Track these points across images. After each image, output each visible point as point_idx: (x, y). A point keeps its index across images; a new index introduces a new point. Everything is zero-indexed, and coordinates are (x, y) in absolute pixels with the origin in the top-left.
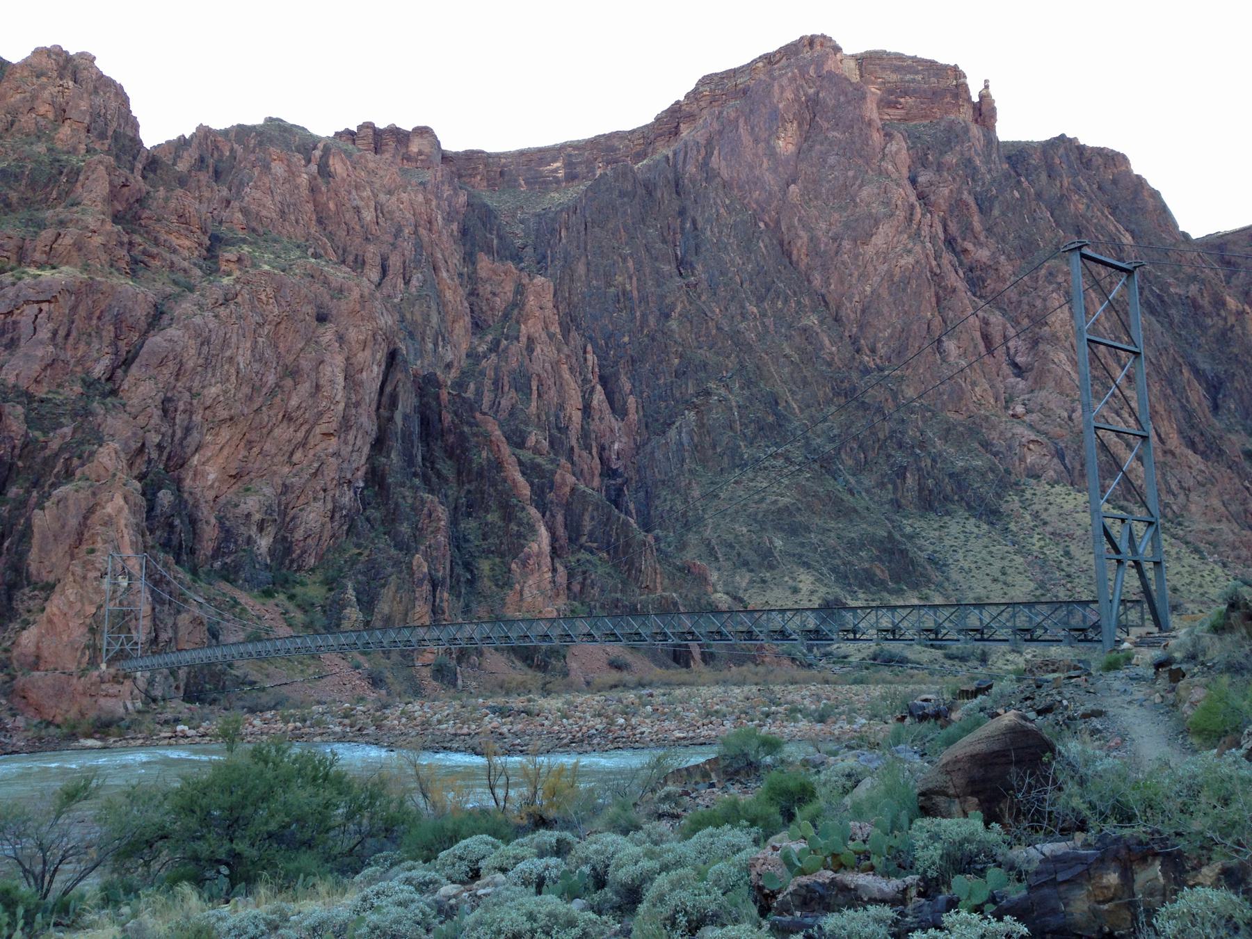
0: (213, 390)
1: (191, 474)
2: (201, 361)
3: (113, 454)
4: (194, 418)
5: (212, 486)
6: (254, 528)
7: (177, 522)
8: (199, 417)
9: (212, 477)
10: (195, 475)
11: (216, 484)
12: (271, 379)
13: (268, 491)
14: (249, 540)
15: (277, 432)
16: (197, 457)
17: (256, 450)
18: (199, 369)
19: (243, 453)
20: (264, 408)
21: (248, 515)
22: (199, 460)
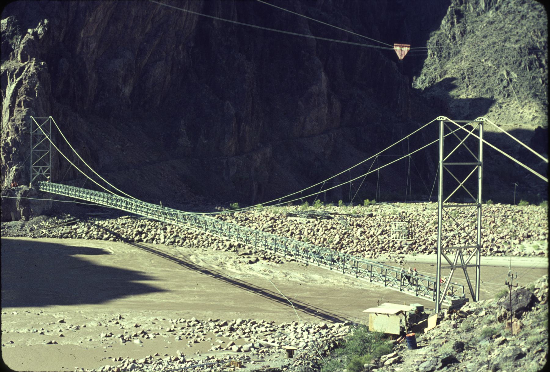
1: (80, 45)
6: (120, 81)
10: (83, 45)
16: (83, 32)
22: (84, 34)
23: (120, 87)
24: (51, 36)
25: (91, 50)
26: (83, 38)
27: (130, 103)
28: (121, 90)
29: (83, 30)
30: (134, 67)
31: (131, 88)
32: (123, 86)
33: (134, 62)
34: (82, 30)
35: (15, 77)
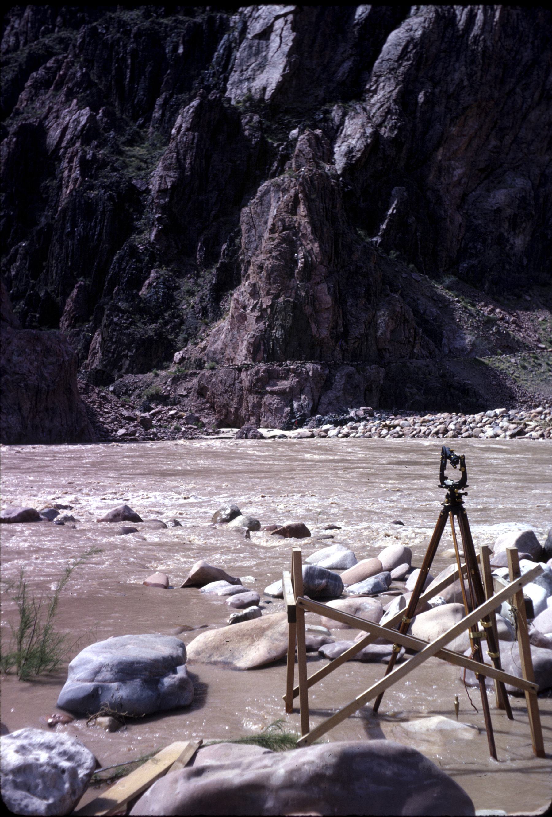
0: (457, 76)
2: (444, 46)
3: (313, 141)
4: (437, 109)
5: (459, 183)
6: (506, 225)
7: (411, 220)
8: (442, 108)
9: (459, 172)
10: (440, 172)
11: (464, 180)
12: (527, 55)
13: (520, 182)
14: (501, 241)
15: (533, 116)
16: (441, 150)
17: (508, 139)
18: (442, 55)
19: (493, 142)
20: (518, 90)
21: (499, 210)
22: (444, 155)
23: (506, 234)
24: (381, 155)
25: (455, 179)
26: (441, 161)
27: (525, 262)
28: (508, 240)
29: (441, 149)
30: (532, 203)
31: (528, 238)
32: (512, 233)
33: (532, 194)
34: (438, 148)
35: (281, 195)
